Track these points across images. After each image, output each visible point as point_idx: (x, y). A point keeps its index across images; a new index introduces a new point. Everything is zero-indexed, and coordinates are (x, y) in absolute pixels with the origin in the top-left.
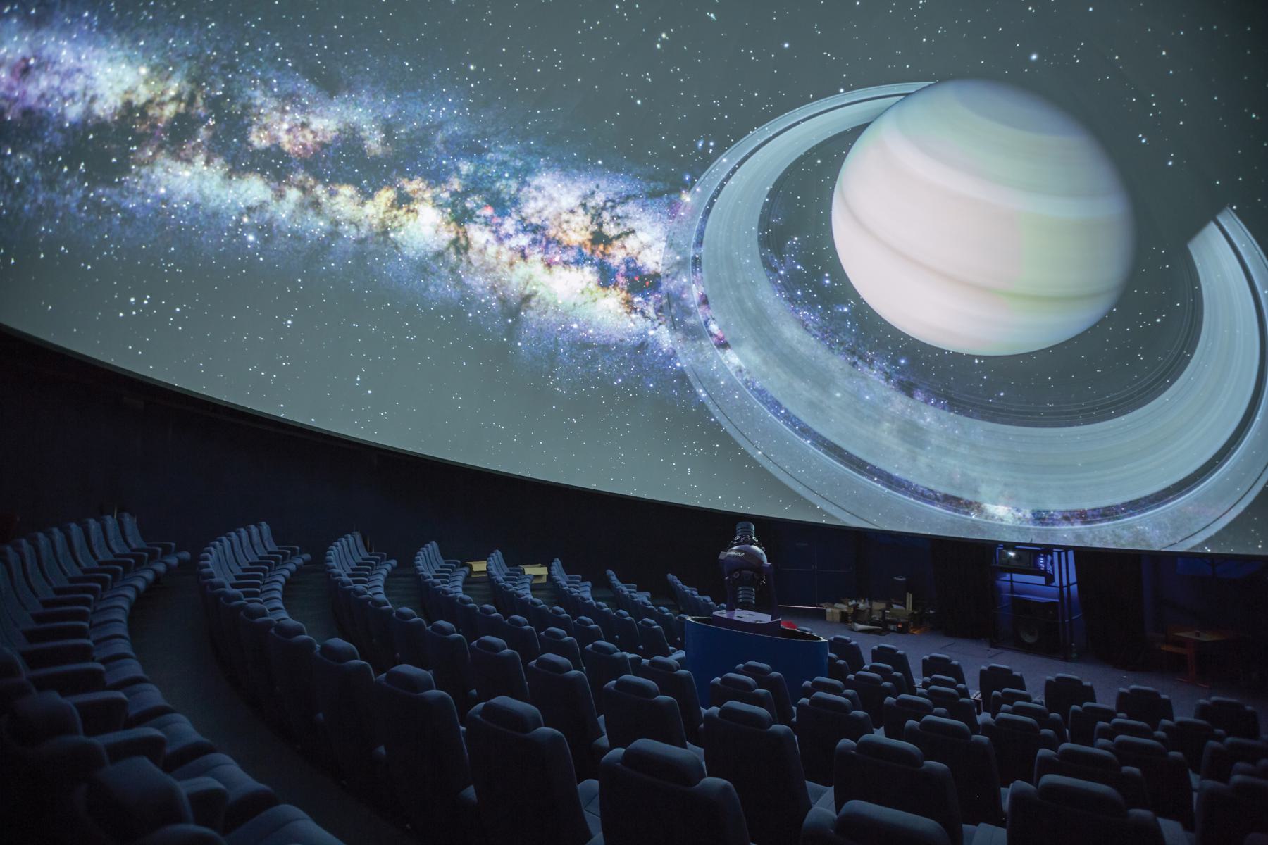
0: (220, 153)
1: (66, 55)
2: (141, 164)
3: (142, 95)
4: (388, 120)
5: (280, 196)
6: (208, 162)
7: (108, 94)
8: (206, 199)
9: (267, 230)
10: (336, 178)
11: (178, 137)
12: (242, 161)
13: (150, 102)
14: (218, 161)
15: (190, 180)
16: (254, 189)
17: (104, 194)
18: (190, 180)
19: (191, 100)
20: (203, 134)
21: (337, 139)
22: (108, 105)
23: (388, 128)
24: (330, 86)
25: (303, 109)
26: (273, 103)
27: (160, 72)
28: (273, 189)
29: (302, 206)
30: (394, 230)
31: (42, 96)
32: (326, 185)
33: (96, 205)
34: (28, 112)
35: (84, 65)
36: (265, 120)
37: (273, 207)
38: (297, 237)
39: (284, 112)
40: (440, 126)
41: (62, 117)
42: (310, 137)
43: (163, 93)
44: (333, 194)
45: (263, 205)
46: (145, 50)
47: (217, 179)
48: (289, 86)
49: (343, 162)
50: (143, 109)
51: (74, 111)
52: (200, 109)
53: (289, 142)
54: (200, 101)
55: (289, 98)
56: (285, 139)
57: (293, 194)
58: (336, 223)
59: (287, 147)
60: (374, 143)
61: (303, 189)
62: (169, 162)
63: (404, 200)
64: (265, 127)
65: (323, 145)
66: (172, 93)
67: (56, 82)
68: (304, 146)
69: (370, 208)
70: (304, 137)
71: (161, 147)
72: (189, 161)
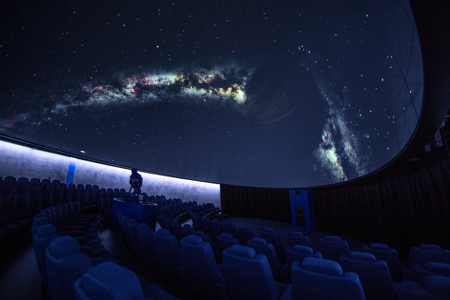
1: (164, 77)
3: (178, 79)
4: (223, 71)
5: (208, 92)
6: (193, 88)
9: (207, 98)
10: (218, 87)
11: (186, 84)
12: (199, 87)
14: (195, 87)
15: (191, 91)
16: (203, 91)
18: (191, 91)
19: (186, 78)
21: (215, 78)
22: (173, 81)
23: (224, 73)
24: (209, 68)
25: (206, 74)
26: (200, 74)
27: (179, 75)
30: (234, 97)
32: (217, 88)
33: (177, 96)
34: (162, 85)
37: (207, 94)
38: (214, 100)
39: (203, 76)
40: (235, 70)
44: (219, 90)
45: (205, 94)
47: (196, 90)
48: (201, 70)
49: (217, 83)
51: (169, 84)
55: (202, 73)
56: (205, 80)
57: (211, 91)
58: (221, 96)
60: (223, 77)
61: (212, 90)
63: (234, 90)
64: (200, 79)
65: (213, 80)
69: (227, 93)
72: (190, 88)
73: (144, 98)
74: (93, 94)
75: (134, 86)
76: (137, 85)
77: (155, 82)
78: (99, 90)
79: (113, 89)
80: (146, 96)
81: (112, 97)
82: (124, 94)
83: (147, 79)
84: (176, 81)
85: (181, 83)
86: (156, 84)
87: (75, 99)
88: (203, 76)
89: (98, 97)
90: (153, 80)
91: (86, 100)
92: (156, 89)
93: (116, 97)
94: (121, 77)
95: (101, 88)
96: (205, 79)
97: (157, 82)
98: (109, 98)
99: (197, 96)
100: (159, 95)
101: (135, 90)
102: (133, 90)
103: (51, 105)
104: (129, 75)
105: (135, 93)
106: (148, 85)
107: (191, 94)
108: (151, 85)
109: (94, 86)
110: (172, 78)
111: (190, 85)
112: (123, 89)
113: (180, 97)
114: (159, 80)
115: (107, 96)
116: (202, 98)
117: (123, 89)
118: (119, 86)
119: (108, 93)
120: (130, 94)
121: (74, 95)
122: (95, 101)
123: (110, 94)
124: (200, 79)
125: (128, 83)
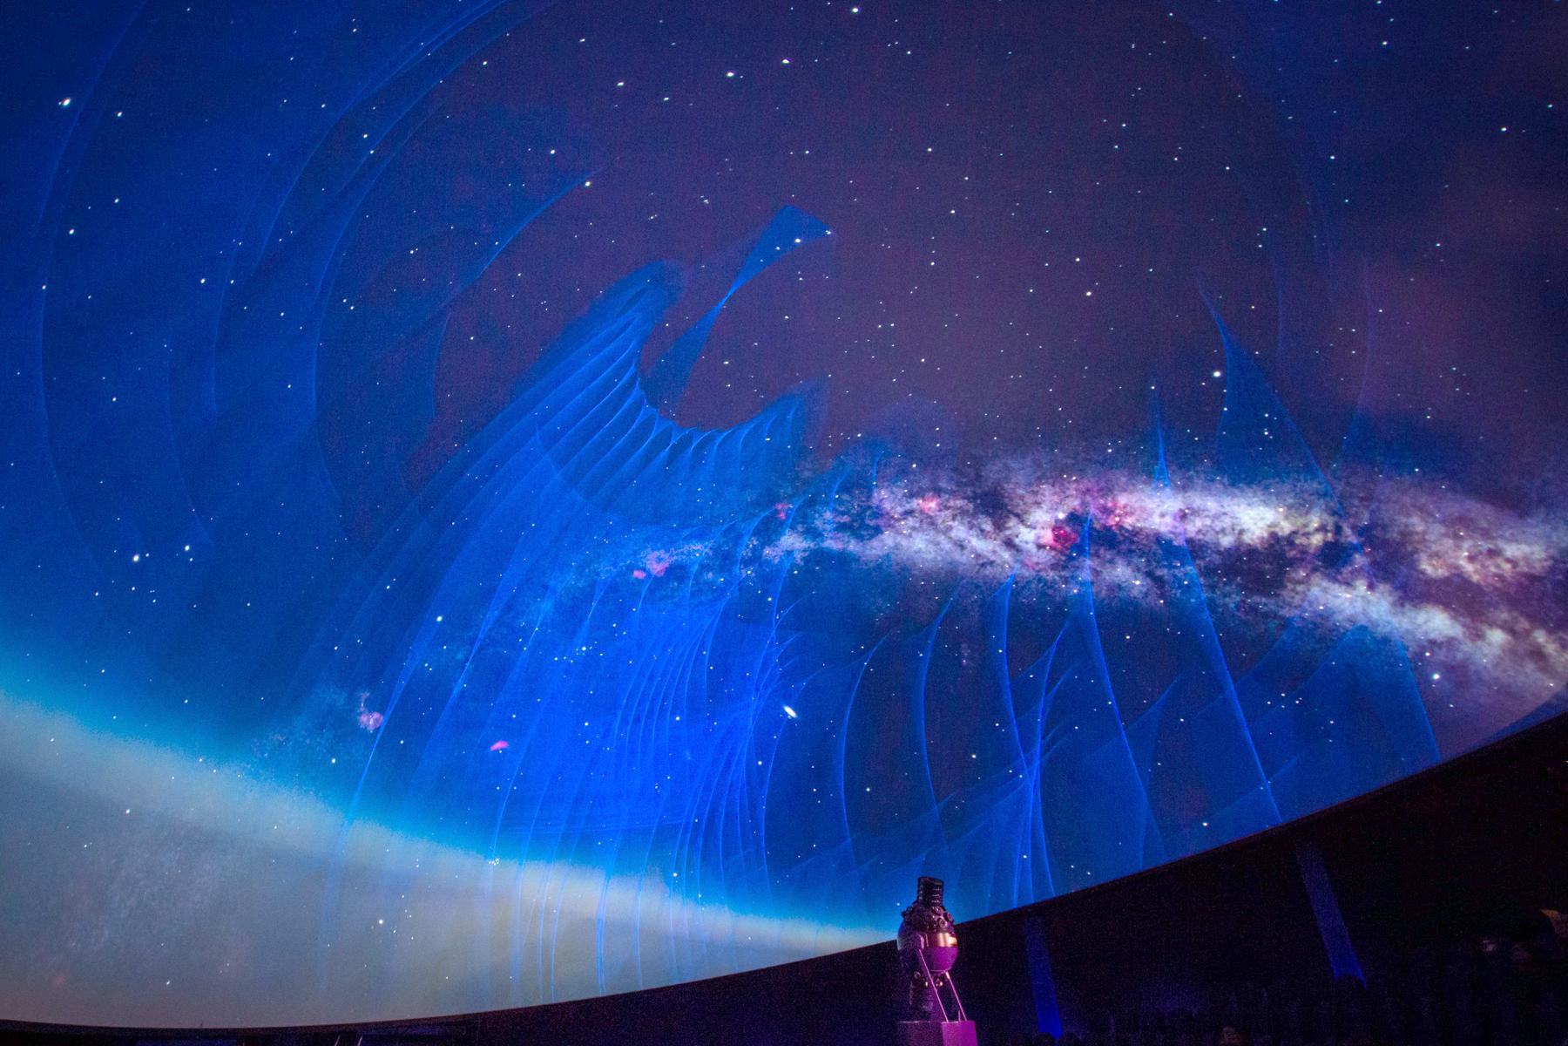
0: (1386, 580)
1: (1211, 504)
2: (1300, 582)
3: (1286, 528)
5: (1478, 636)
6: (1371, 587)
7: (1253, 528)
8: (1375, 624)
9: (1459, 672)
11: (1333, 559)
12: (1414, 592)
13: (1294, 533)
14: (1383, 588)
15: (1354, 601)
16: (1436, 622)
17: (1262, 602)
19: (1338, 530)
20: (1359, 560)
25: (1486, 534)
28: (1464, 625)
29: (1510, 651)
31: (1199, 531)
33: (1253, 609)
34: (1189, 541)
35: (1227, 509)
36: (1434, 548)
38: (1506, 691)
41: (1217, 544)
42: (1508, 567)
43: (1305, 526)
45: (1450, 643)
46: (1277, 495)
50: (1290, 540)
51: (1227, 541)
52: (1350, 536)
53: (1476, 572)
54: (1347, 530)
55: (1459, 524)
56: (1469, 568)
59: (1475, 578)
61: (1510, 630)
62: (1325, 583)
64: (1437, 555)
65: (1533, 578)
66: (1315, 525)
67: (1208, 522)
68: (1501, 577)
70: (1498, 566)
71: (1315, 570)
73: (1085, 575)
74: (898, 520)
75: (1057, 521)
76: (1073, 518)
77: (1157, 520)
78: (922, 512)
79: (974, 515)
80: (1096, 573)
81: (961, 545)
82: (1009, 544)
83: (1123, 500)
84: (1273, 535)
85: (1304, 551)
86: (1163, 529)
87: (842, 527)
88: (1456, 537)
89: (910, 536)
90: (1154, 508)
91: (872, 537)
92: (1157, 551)
93: (974, 551)
94: (1019, 477)
95: (933, 505)
96: (1471, 559)
97: (1168, 520)
98: (947, 546)
99: (1386, 640)
100: (1159, 582)
101: (1057, 538)
102: (1048, 536)
103: (768, 532)
104: (1056, 475)
105: (1052, 548)
106: (1120, 526)
107: (1351, 620)
108: (1136, 532)
109: (912, 495)
110: (1254, 517)
111: (1356, 573)
112: (1012, 522)
113: (1276, 616)
114: (1183, 516)
115: (941, 538)
116: (1420, 656)
117: (1012, 522)
118: (995, 507)
119: (950, 528)
120: (1032, 547)
121: (843, 513)
122: (897, 547)
123: (953, 534)
124: (1437, 555)
125: (1038, 504)
